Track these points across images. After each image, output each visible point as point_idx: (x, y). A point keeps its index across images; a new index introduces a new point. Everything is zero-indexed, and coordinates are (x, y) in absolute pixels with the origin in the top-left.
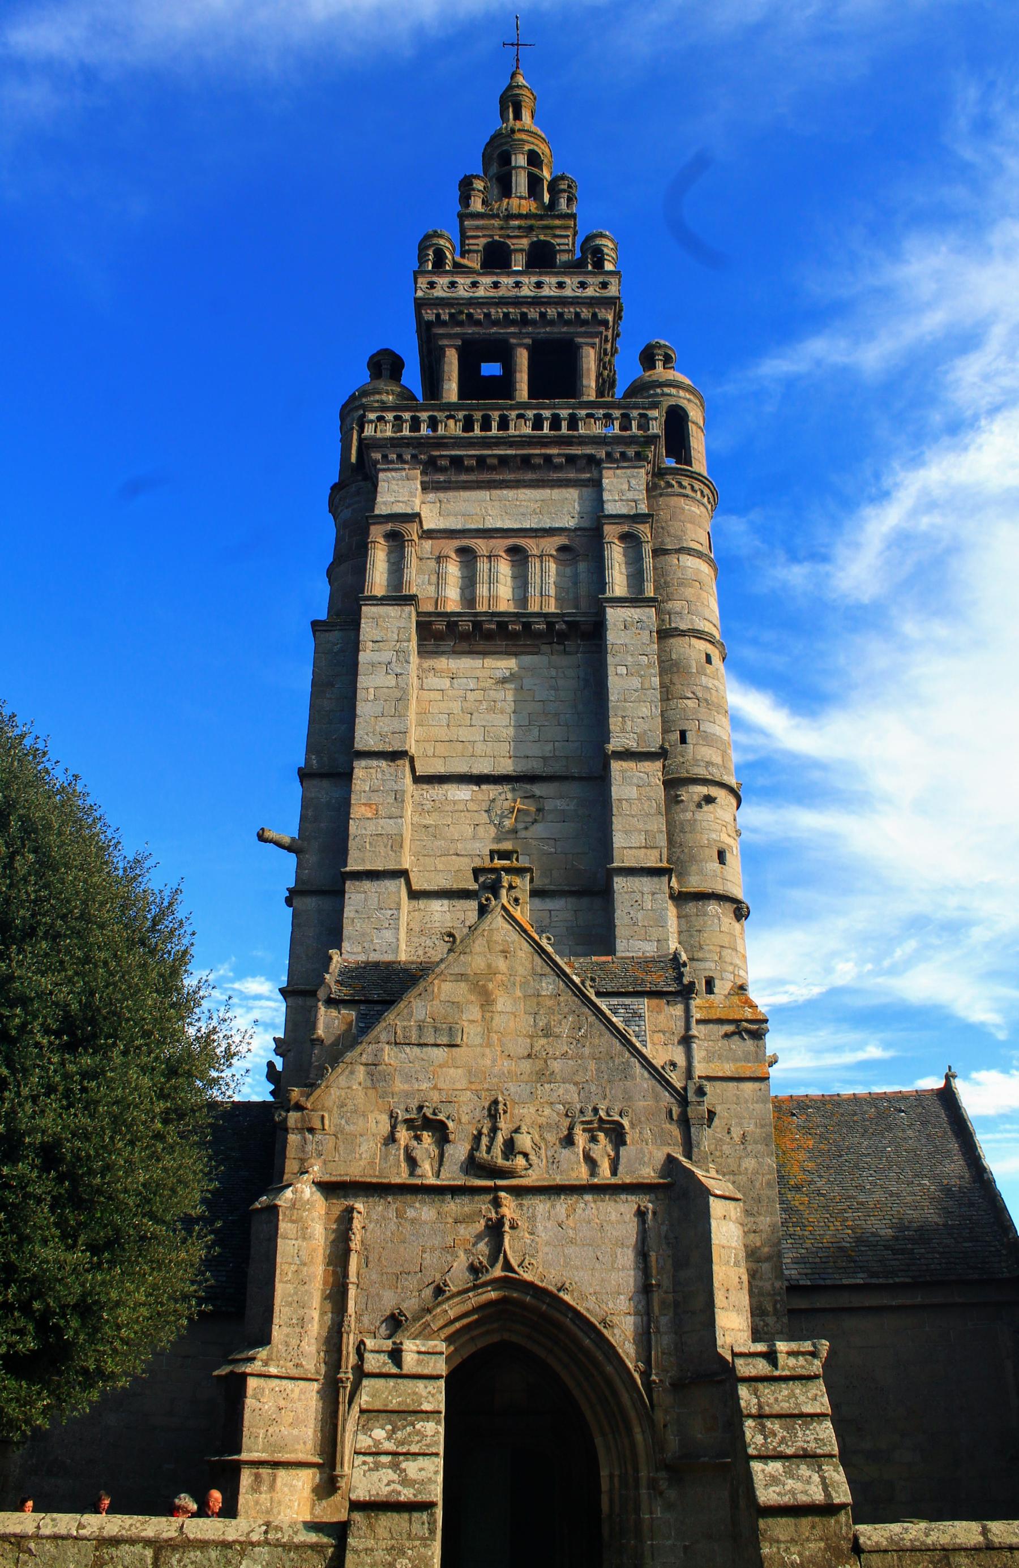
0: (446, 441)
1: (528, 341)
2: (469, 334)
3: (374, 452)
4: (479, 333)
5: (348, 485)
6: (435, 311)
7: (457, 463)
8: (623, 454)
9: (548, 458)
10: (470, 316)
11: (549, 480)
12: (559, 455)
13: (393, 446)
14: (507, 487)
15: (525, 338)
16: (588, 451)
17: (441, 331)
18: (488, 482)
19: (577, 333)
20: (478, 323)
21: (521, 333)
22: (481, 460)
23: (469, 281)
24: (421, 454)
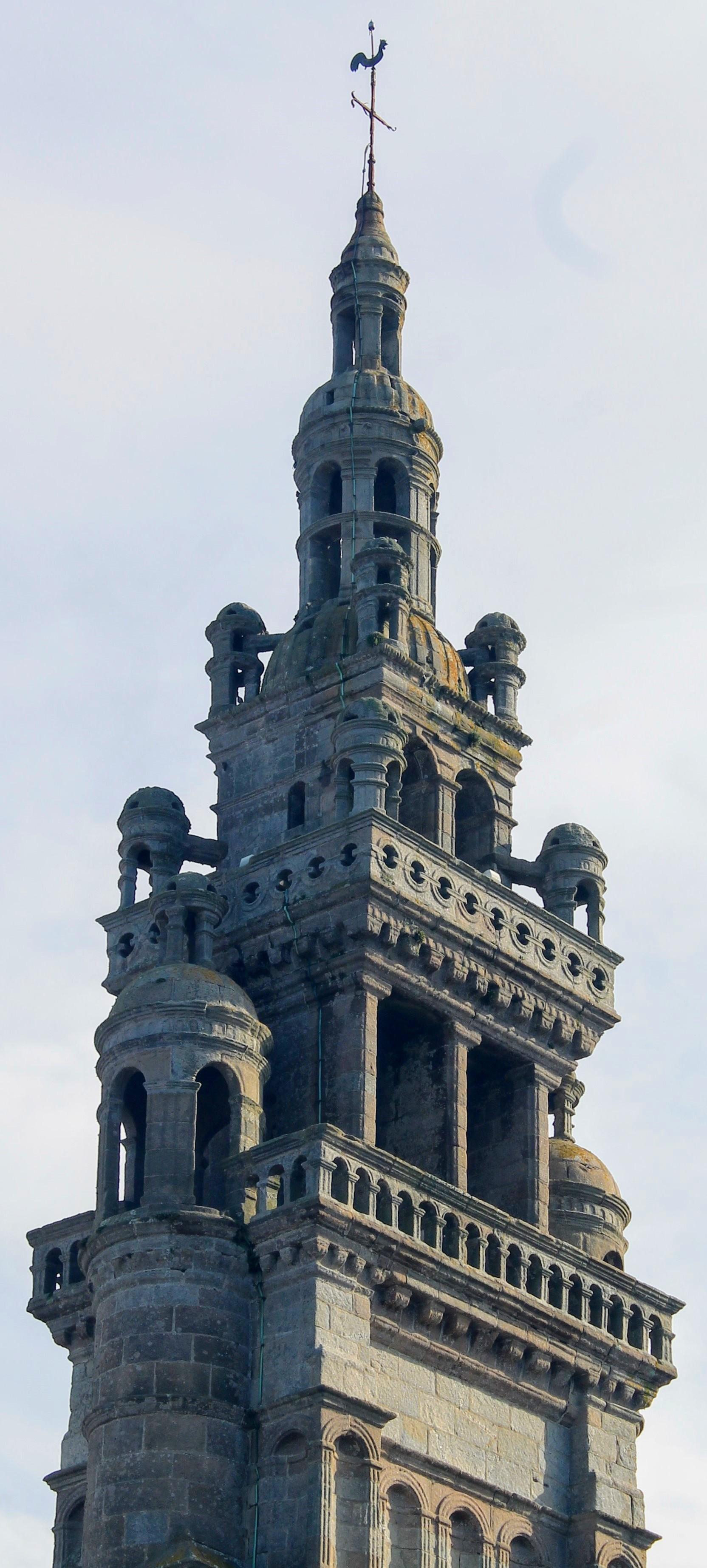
0: (423, 1261)
1: (477, 1038)
2: (410, 984)
3: (322, 1234)
4: (422, 990)
5: (201, 1234)
6: (385, 918)
7: (419, 1301)
8: (620, 1386)
9: (530, 1350)
10: (426, 951)
11: (516, 1389)
12: (548, 1353)
13: (352, 1237)
14: (460, 1377)
15: (476, 1029)
16: (585, 1362)
17: (378, 958)
18: (441, 1357)
19: (543, 1056)
20: (428, 970)
21: (474, 1018)
22: (450, 1314)
23: (440, 873)
24: (380, 1267)
